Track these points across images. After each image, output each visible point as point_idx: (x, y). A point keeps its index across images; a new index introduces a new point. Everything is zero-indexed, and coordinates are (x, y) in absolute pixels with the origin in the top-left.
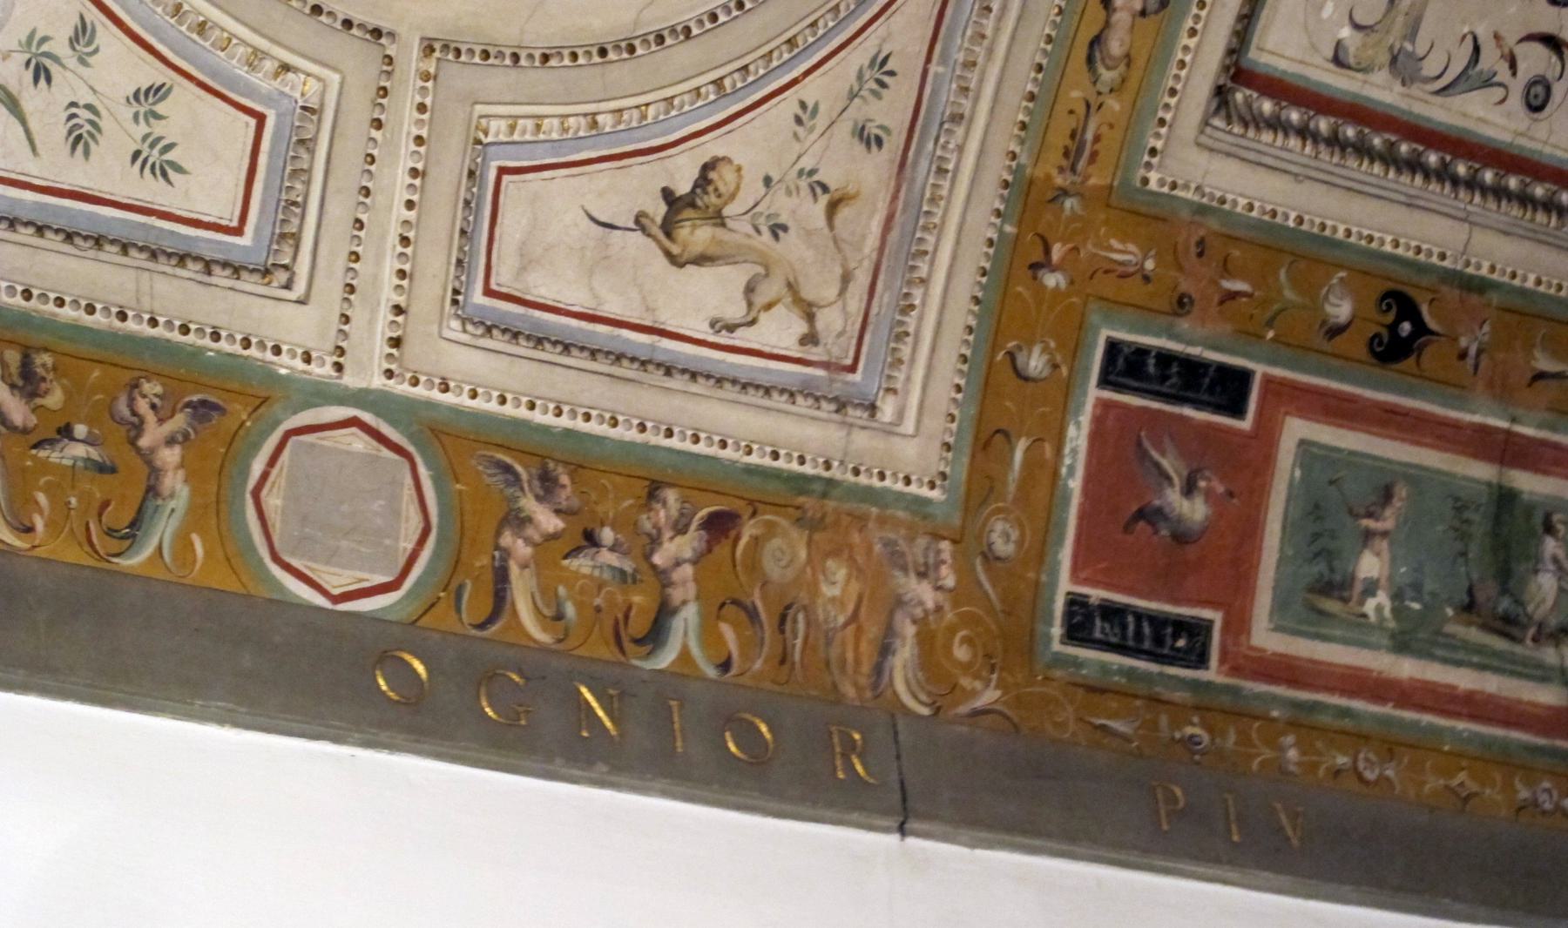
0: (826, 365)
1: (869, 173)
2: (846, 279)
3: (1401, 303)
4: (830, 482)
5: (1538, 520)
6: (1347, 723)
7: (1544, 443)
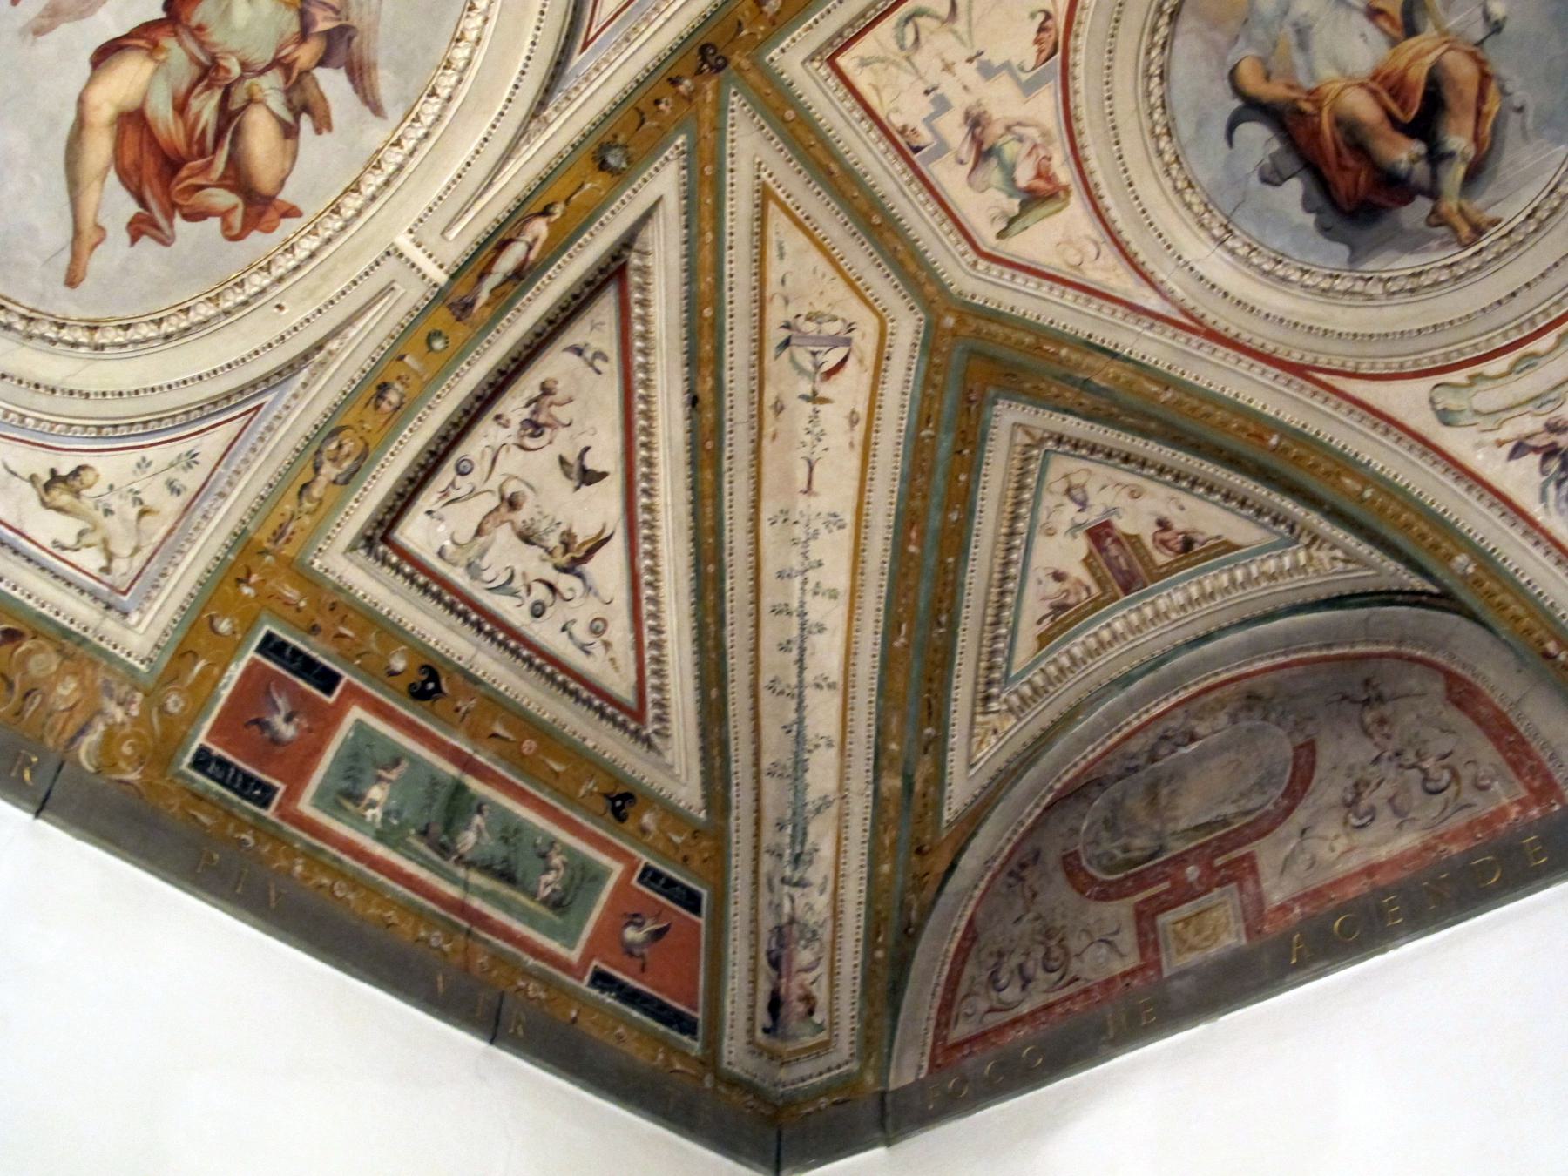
0: (111, 587)
1: (170, 506)
2: (137, 550)
3: (432, 673)
4: (85, 640)
5: (474, 805)
6: (335, 865)
7: (487, 768)
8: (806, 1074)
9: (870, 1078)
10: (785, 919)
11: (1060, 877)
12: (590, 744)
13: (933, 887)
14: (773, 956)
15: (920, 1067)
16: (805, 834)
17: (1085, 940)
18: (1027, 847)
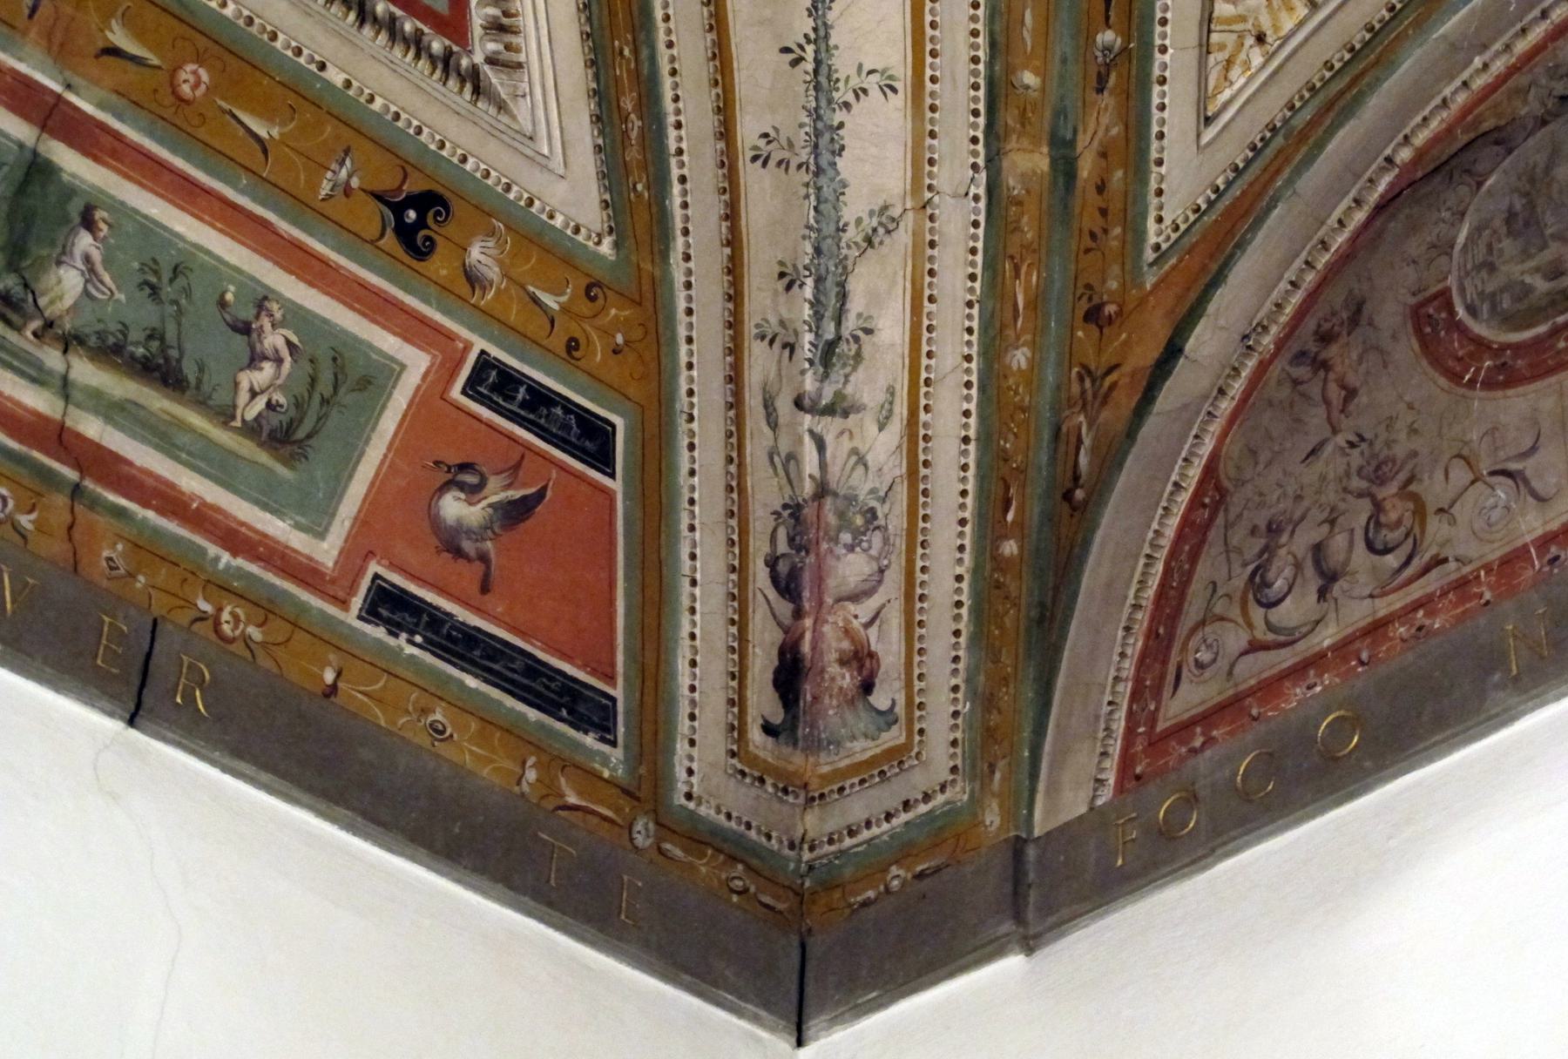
5: (75, 209)
7: (102, 126)
8: (861, 816)
9: (992, 817)
10: (808, 488)
11: (1406, 349)
12: (335, 77)
13: (1125, 401)
14: (783, 568)
15: (1100, 782)
16: (843, 296)
17: (1460, 475)
18: (1336, 297)
